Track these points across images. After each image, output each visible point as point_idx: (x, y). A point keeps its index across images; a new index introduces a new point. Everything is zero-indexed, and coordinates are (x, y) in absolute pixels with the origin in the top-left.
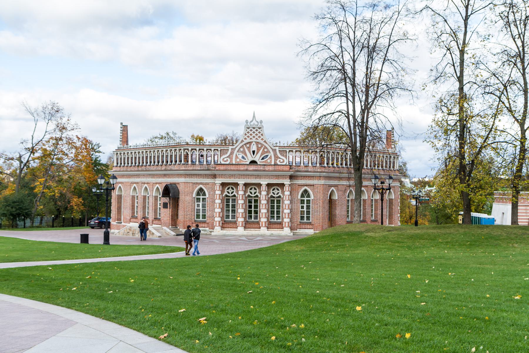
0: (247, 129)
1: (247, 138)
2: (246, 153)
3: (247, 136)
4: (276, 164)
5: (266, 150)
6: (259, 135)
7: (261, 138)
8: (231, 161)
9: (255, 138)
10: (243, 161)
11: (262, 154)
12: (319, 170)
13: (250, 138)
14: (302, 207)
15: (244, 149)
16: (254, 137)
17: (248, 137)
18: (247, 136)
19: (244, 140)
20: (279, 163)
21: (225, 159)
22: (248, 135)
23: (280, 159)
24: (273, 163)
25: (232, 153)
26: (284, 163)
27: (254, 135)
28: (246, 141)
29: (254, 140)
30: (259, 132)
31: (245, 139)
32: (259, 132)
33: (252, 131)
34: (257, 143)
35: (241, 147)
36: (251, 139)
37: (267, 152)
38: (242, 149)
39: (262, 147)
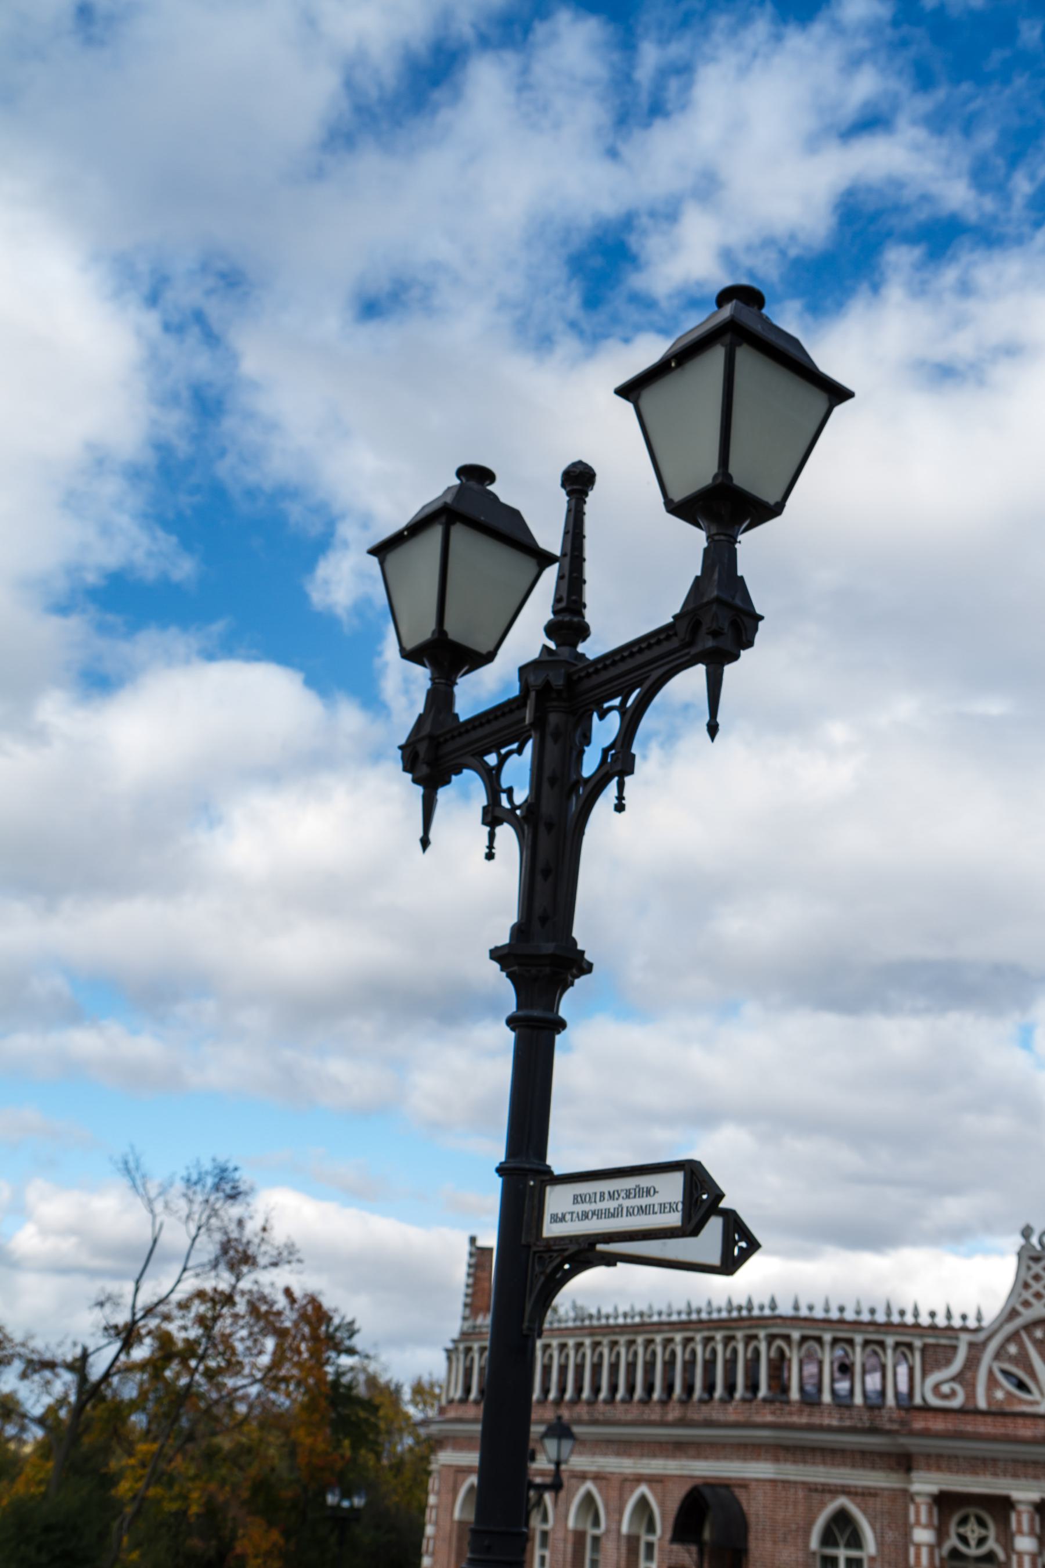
0: (1032, 1264)
1: (1033, 1300)
3: (1032, 1291)
8: (971, 1395)
10: (1021, 1401)
15: (1022, 1347)
18: (1032, 1291)
19: (1020, 1309)
21: (945, 1389)
25: (972, 1362)
31: (1026, 1304)
35: (1009, 1339)
38: (1013, 1349)
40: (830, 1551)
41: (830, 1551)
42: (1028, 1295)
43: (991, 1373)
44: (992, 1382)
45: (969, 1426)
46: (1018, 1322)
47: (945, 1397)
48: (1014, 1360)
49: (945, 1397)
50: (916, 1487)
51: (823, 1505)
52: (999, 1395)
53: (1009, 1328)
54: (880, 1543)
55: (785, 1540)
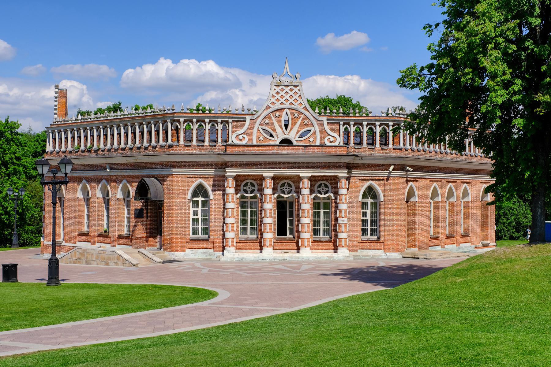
0: (275, 88)
1: (275, 102)
2: (274, 127)
4: (323, 146)
5: (306, 122)
6: (296, 97)
7: (298, 103)
8: (250, 138)
9: (289, 102)
13: (280, 102)
15: (271, 120)
16: (287, 100)
17: (278, 100)
18: (275, 98)
20: (328, 144)
21: (241, 137)
22: (278, 97)
23: (330, 137)
25: (251, 127)
26: (336, 144)
27: (287, 97)
28: (274, 108)
29: (287, 105)
30: (296, 93)
31: (273, 103)
32: (296, 93)
33: (284, 92)
36: (282, 103)
37: (307, 125)
39: (300, 117)
40: (195, 199)
41: (195, 199)
42: (273, 100)
43: (258, 130)
44: (259, 134)
46: (270, 110)
47: (241, 140)
49: (241, 140)
50: (227, 174)
51: (193, 182)
53: (266, 113)
55: (178, 196)
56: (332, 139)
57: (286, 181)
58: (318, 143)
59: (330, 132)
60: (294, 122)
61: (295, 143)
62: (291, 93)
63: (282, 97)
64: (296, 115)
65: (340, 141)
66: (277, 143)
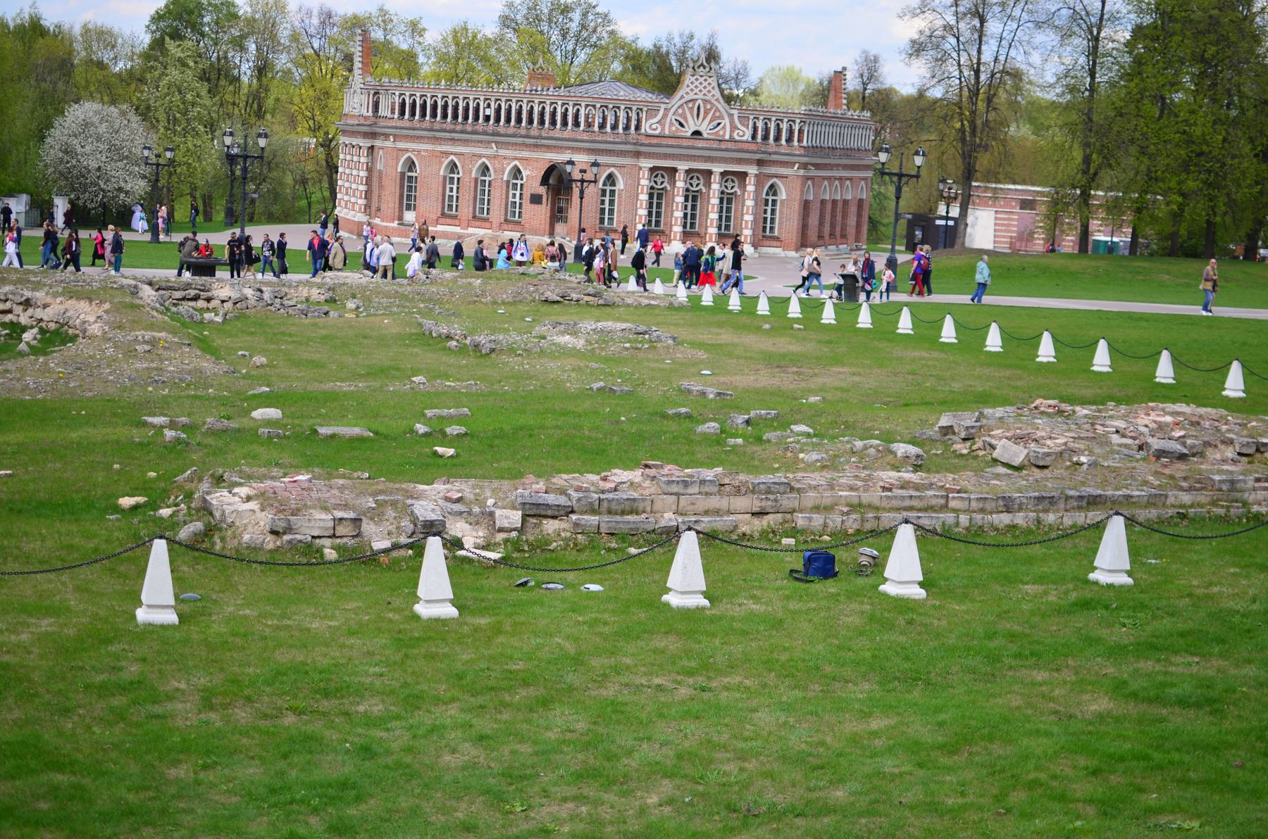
4: (732, 140)
5: (717, 114)
6: (709, 88)
8: (663, 129)
11: (711, 121)
12: (797, 152)
14: (765, 212)
15: (684, 110)
16: (700, 91)
17: (692, 90)
20: (737, 138)
21: (654, 126)
24: (727, 137)
25: (665, 116)
26: (745, 138)
27: (701, 87)
28: (687, 98)
30: (709, 84)
31: (687, 93)
34: (705, 101)
37: (718, 118)
38: (680, 111)
45: (664, 142)
48: (681, 115)
52: (674, 128)
53: (680, 103)
54: (626, 184)
56: (741, 133)
57: (695, 174)
58: (727, 137)
59: (740, 126)
60: (706, 113)
61: (705, 135)
62: (705, 84)
63: (696, 87)
64: (709, 107)
65: (748, 137)
66: (689, 134)
